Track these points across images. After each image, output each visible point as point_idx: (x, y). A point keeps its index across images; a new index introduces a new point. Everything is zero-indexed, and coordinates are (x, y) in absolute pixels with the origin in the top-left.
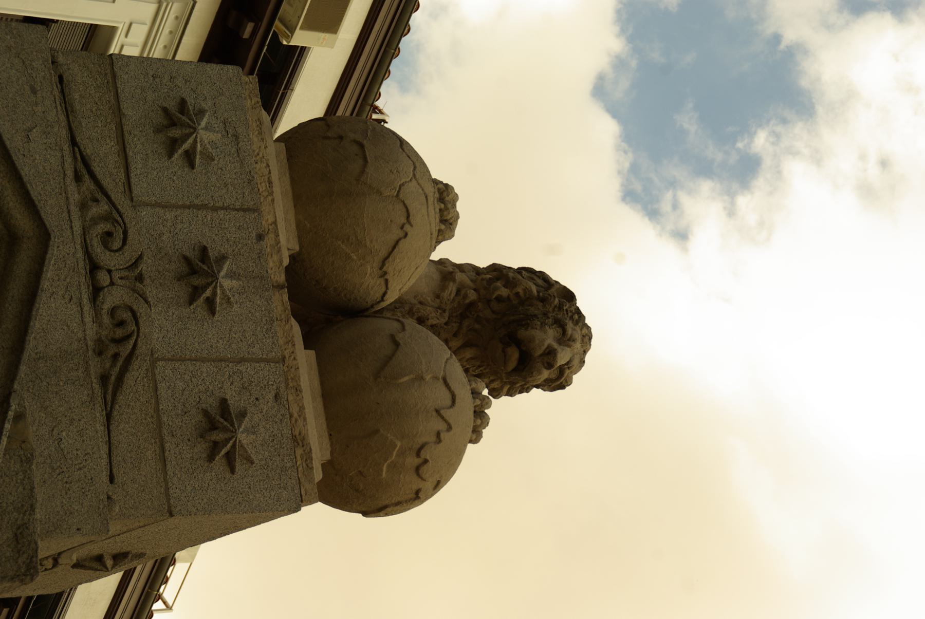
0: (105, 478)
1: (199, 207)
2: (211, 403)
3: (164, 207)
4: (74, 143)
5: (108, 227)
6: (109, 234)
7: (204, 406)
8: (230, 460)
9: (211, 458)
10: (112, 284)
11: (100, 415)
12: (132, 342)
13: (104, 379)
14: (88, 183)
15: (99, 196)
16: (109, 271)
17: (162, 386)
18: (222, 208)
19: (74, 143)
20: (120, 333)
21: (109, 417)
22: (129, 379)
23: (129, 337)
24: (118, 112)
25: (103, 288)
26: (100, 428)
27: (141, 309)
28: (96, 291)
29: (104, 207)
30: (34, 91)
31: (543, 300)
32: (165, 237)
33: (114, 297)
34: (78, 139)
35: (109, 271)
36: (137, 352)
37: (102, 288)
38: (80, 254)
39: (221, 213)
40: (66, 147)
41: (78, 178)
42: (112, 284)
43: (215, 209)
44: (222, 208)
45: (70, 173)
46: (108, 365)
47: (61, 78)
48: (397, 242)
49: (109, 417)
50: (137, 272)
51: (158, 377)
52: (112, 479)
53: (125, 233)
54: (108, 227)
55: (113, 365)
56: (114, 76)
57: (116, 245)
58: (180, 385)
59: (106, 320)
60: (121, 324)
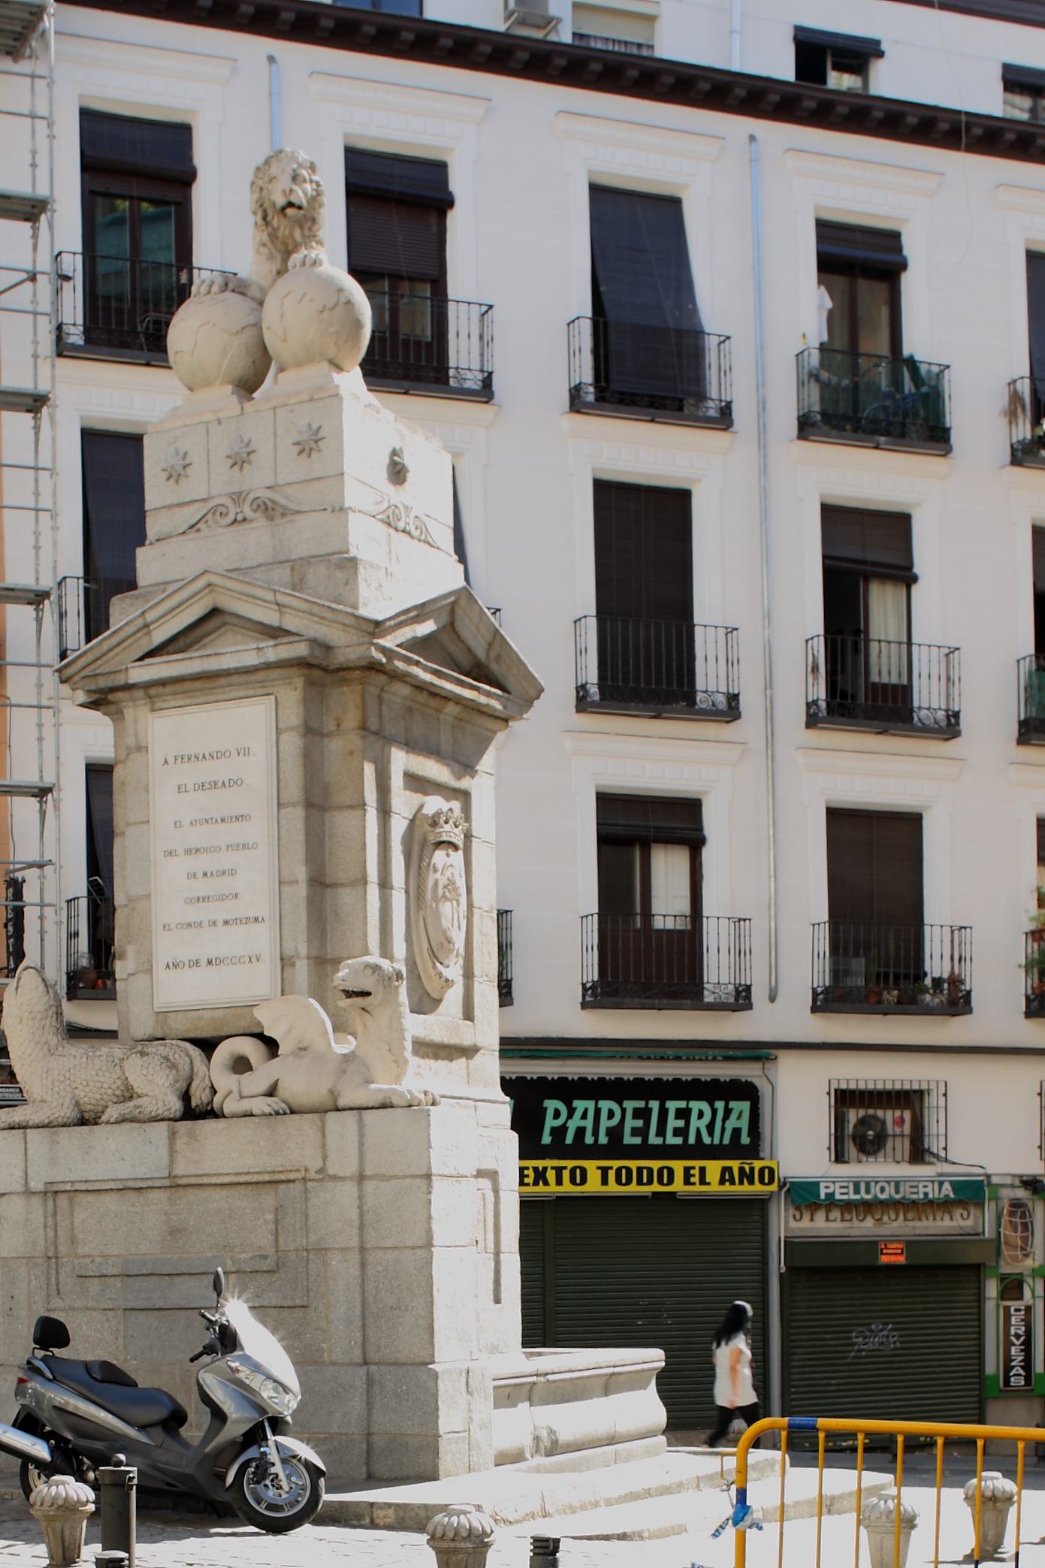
14: (201, 525)
15: (205, 519)
16: (237, 513)
19: (184, 533)
20: (263, 507)
23: (265, 503)
24: (170, 507)
27: (252, 496)
33: (248, 512)
35: (237, 513)
40: (186, 537)
41: (198, 530)
47: (158, 540)
52: (325, 510)
53: (220, 505)
56: (155, 509)
57: (224, 510)
60: (259, 506)
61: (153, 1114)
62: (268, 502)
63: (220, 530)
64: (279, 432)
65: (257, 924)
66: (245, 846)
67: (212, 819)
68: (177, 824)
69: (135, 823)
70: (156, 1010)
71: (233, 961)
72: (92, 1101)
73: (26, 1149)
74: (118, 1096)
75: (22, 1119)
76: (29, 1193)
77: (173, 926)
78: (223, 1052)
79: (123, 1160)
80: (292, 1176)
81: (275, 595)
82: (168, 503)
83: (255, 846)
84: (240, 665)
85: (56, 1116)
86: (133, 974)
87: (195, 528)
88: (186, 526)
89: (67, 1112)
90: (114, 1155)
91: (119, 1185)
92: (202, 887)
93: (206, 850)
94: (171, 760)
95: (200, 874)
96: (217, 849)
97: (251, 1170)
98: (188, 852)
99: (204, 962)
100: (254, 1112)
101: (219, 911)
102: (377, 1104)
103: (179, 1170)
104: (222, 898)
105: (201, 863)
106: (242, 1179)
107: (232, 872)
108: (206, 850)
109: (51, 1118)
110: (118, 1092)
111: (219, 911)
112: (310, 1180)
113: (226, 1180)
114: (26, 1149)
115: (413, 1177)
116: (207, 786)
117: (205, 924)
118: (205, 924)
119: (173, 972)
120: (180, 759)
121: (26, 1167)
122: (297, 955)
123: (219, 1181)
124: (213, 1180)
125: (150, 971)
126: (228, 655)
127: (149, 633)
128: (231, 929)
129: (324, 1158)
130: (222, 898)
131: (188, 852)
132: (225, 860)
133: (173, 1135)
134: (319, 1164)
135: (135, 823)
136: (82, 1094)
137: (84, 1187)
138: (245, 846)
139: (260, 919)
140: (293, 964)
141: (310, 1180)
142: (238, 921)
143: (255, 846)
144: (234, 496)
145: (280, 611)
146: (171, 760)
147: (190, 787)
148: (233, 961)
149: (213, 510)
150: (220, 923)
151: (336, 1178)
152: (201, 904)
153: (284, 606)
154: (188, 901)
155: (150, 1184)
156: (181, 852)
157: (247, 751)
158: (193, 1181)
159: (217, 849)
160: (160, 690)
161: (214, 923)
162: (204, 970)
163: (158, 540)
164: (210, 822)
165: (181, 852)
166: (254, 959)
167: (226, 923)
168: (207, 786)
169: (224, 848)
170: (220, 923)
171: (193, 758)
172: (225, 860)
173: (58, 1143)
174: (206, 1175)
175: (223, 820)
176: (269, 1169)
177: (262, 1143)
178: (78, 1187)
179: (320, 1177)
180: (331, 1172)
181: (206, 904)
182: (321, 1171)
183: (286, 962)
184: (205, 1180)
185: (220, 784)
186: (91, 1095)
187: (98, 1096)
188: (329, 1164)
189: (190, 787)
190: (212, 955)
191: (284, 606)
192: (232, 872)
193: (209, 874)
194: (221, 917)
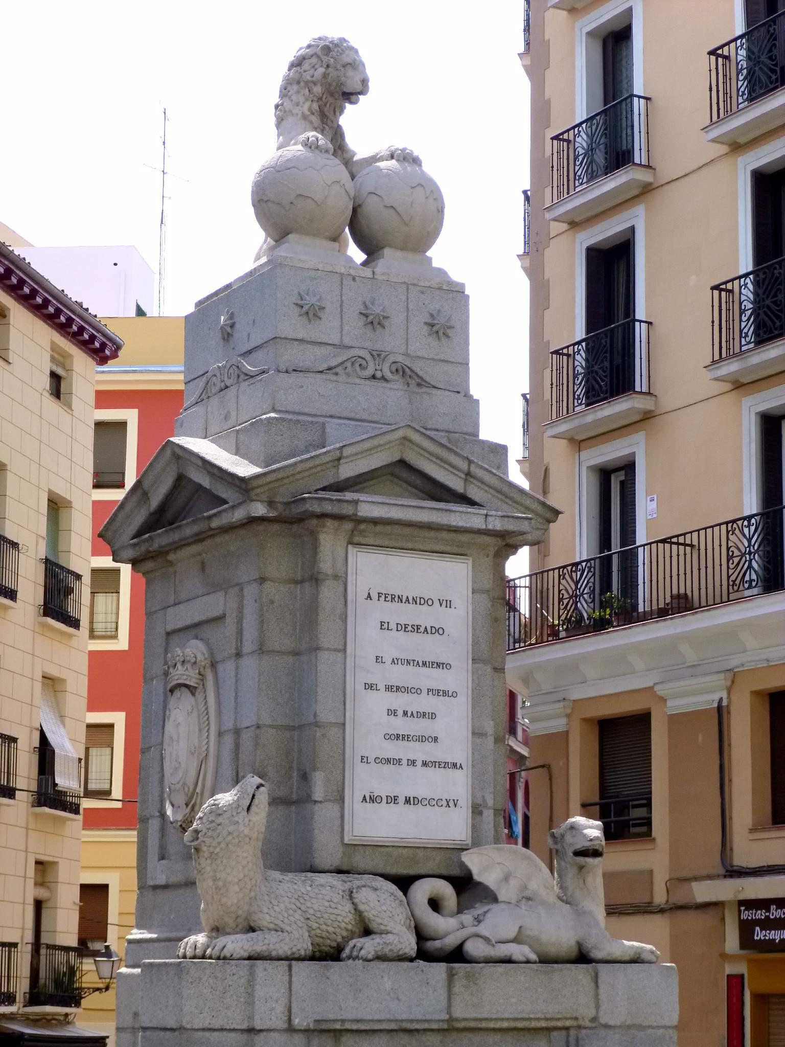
0: (456, 395)
1: (342, 311)
2: (426, 329)
3: (342, 330)
4: (321, 372)
5: (357, 365)
6: (360, 365)
7: (427, 334)
8: (450, 327)
9: (448, 337)
10: (381, 370)
11: (434, 391)
12: (404, 367)
13: (419, 385)
14: (339, 370)
15: (344, 366)
17: (419, 354)
18: (341, 296)
19: (321, 372)
21: (434, 387)
22: (421, 373)
23: (402, 367)
25: (383, 375)
26: (439, 392)
27: (392, 358)
28: (384, 378)
29: (348, 364)
30: (302, 387)
31: (328, 66)
32: (356, 333)
34: (321, 370)
36: (409, 366)
37: (383, 376)
38: (367, 382)
39: (344, 298)
40: (324, 376)
41: (336, 374)
42: (381, 370)
43: (342, 301)
44: (341, 296)
45: (335, 378)
46: (413, 381)
47: (294, 370)
48: (346, 190)
49: (434, 387)
50: (376, 356)
51: (415, 355)
52: (458, 392)
53: (360, 357)
54: (357, 365)
55: (414, 379)
56: (286, 338)
57: (364, 363)
58: (418, 344)
59: (396, 377)
61: (401, 953)
62: (407, 370)
63: (357, 381)
64: (411, 308)
65: (455, 770)
66: (445, 693)
67: (414, 661)
68: (379, 659)
69: (328, 649)
70: (346, 841)
71: (430, 802)
72: (324, 934)
73: (290, 983)
74: (347, 930)
75: (264, 948)
76: (291, 1029)
77: (371, 759)
78: (422, 890)
79: (398, 999)
80: (568, 1023)
81: (469, 466)
82: (300, 336)
83: (454, 695)
84: (468, 526)
85: (299, 947)
86: (321, 802)
87: (334, 371)
88: (325, 366)
89: (304, 946)
90: (389, 994)
91: (393, 1026)
92: (401, 725)
93: (407, 690)
94: (374, 596)
95: (400, 713)
96: (418, 691)
97: (532, 1016)
98: (389, 688)
99: (402, 800)
100: (514, 957)
101: (419, 752)
102: (627, 958)
103: (458, 1013)
104: (422, 739)
105: (400, 701)
106: (520, 1025)
107: (433, 716)
108: (407, 690)
109: (294, 950)
110: (350, 927)
111: (419, 752)
112: (585, 1028)
113: (505, 1025)
114: (290, 983)
115: (666, 1027)
116: (410, 628)
117: (404, 762)
118: (404, 762)
119: (369, 806)
120: (383, 597)
121: (290, 1002)
122: (486, 806)
123: (498, 1025)
124: (492, 1025)
125: (341, 800)
126: (458, 514)
127: (337, 467)
128: (430, 771)
129: (598, 1007)
130: (422, 739)
131: (389, 688)
132: (425, 703)
133: (451, 976)
134: (592, 1013)
135: (328, 649)
136: (315, 925)
137: (355, 1027)
138: (445, 693)
139: (458, 766)
140: (481, 813)
141: (585, 1028)
142: (437, 764)
143: (454, 695)
144: (374, 353)
145: (466, 480)
146: (374, 596)
147: (393, 626)
148: (430, 802)
149: (353, 360)
150: (419, 763)
151: (607, 1026)
152: (400, 742)
153: (472, 476)
154: (387, 737)
155: (426, 1026)
156: (381, 687)
157: (449, 604)
158: (472, 1024)
159: (418, 691)
160: (371, 527)
161: (413, 763)
162: (401, 807)
163: (294, 370)
164: (412, 664)
165: (381, 687)
166: (451, 803)
167: (425, 764)
168: (410, 628)
169: (425, 691)
170: (419, 763)
171: (396, 599)
172: (425, 703)
173: (328, 978)
174: (486, 1019)
175: (424, 664)
176: (549, 1016)
177: (540, 990)
178: (348, 1026)
179: (594, 1025)
180: (603, 1021)
181: (405, 743)
182: (594, 1019)
183: (477, 810)
184: (484, 1025)
185: (422, 629)
186: (324, 927)
187: (331, 929)
188: (601, 1013)
189: (393, 626)
190: (411, 794)
191: (472, 476)
192: (433, 716)
193: (409, 714)
194: (420, 758)
